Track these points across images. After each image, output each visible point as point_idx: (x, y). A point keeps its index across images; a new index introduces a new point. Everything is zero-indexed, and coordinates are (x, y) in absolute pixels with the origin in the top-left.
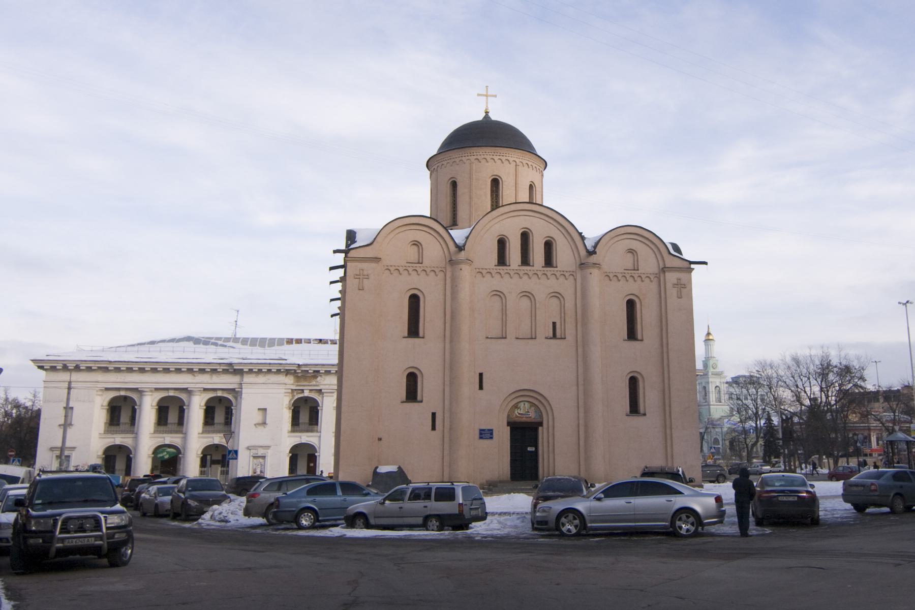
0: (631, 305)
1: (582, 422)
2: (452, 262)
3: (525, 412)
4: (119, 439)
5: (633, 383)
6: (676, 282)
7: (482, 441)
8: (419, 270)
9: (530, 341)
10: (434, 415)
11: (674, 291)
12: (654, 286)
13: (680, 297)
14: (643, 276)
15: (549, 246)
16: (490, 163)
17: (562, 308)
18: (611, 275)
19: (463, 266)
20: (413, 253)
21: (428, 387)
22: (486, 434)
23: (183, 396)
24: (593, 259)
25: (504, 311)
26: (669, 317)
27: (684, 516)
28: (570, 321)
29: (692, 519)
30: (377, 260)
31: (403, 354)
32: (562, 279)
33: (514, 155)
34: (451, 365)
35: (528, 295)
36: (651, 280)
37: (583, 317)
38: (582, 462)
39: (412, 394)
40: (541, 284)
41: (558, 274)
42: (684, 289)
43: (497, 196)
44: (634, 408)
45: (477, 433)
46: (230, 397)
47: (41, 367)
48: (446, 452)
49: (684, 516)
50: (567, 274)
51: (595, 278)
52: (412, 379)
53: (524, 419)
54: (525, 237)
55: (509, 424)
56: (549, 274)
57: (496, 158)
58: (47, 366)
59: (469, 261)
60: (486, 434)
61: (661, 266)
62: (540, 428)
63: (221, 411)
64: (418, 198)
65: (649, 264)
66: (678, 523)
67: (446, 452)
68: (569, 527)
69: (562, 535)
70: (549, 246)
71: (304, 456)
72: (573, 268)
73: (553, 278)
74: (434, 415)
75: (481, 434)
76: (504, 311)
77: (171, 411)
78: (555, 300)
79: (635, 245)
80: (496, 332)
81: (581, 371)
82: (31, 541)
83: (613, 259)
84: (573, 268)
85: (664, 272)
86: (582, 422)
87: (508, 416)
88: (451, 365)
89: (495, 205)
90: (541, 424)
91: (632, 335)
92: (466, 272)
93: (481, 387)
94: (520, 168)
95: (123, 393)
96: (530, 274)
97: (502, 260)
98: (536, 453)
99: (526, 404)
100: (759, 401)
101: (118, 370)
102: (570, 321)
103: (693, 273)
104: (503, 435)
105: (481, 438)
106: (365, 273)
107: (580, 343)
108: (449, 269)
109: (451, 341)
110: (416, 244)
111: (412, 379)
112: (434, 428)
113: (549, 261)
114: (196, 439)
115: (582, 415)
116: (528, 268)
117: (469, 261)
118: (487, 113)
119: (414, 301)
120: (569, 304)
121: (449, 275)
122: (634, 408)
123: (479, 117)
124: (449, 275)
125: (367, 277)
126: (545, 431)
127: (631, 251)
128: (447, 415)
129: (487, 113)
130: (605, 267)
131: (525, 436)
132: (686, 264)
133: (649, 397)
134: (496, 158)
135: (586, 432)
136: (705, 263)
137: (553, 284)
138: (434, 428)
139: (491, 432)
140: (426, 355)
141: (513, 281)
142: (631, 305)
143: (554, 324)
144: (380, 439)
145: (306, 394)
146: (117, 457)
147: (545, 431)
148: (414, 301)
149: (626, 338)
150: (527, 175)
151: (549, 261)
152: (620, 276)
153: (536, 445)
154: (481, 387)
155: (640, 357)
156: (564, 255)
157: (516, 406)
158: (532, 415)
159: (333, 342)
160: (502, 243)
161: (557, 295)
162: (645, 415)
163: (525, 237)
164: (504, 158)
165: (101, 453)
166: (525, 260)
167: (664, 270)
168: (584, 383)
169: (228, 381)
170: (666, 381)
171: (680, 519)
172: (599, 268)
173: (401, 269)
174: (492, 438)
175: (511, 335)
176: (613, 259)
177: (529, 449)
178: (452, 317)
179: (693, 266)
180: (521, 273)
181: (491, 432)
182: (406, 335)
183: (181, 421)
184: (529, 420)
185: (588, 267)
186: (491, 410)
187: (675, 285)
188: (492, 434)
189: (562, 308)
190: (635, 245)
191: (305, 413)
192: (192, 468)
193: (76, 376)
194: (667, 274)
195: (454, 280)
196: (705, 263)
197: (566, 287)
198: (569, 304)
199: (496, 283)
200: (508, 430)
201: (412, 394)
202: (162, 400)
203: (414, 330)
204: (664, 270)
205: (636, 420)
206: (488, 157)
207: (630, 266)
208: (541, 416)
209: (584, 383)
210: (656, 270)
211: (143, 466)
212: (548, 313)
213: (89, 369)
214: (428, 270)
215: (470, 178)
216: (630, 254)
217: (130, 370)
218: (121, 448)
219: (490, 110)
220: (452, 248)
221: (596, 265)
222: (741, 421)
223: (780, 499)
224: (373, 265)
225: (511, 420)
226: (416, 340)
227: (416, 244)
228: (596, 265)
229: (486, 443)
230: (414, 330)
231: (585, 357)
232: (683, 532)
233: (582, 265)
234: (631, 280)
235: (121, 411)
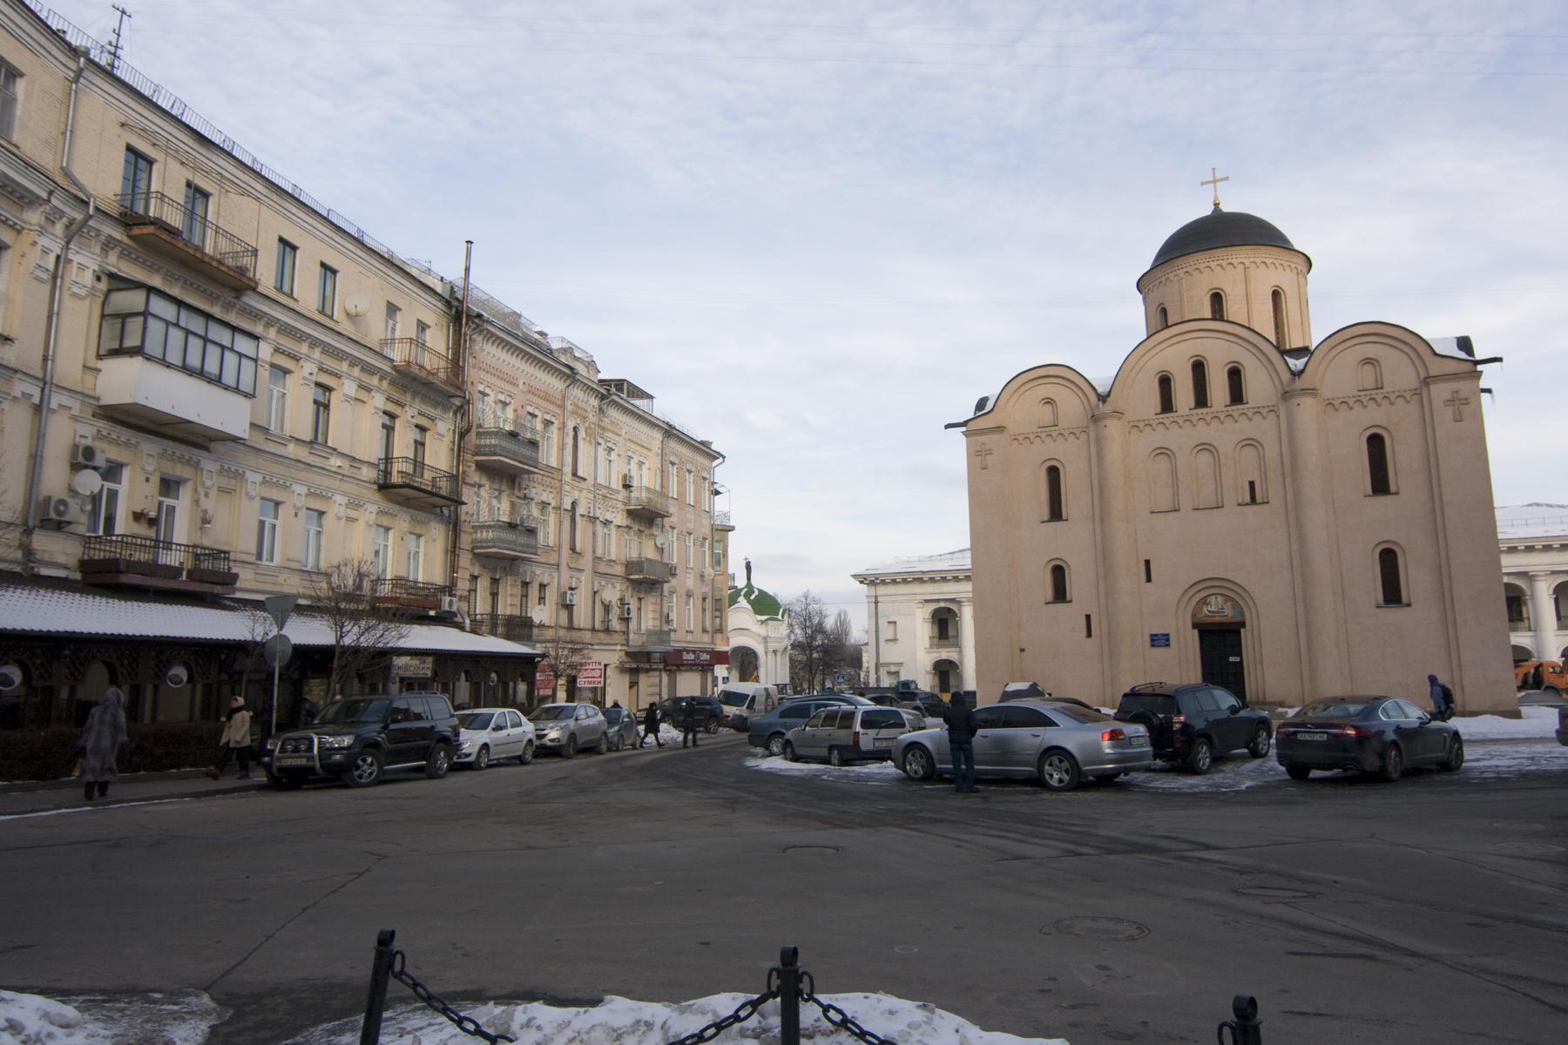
1: (1301, 619)
2: (1095, 419)
6: (1449, 396)
10: (1088, 617)
12: (1413, 408)
14: (1392, 397)
15: (1235, 375)
17: (1261, 458)
18: (1336, 403)
19: (1108, 422)
22: (1161, 640)
25: (1174, 475)
30: (1000, 429)
31: (1042, 543)
32: (1257, 418)
35: (1205, 447)
36: (1424, 395)
37: (1292, 468)
39: (1060, 593)
45: (1148, 639)
50: (1264, 411)
51: (1306, 409)
52: (1059, 573)
53: (1217, 619)
54: (1199, 368)
55: (1195, 626)
56: (1236, 414)
59: (1118, 414)
60: (1161, 640)
61: (1423, 375)
65: (1400, 374)
70: (1235, 375)
72: (1274, 401)
73: (1243, 421)
74: (1088, 617)
76: (1174, 475)
79: (1372, 351)
80: (1167, 505)
83: (1339, 377)
84: (1274, 401)
85: (1428, 384)
87: (1194, 615)
90: (1243, 624)
92: (1113, 428)
93: (1149, 579)
96: (1208, 418)
97: (1167, 405)
98: (1241, 662)
99: (1220, 599)
108: (1092, 427)
110: (1049, 401)
111: (1059, 573)
112: (1089, 635)
113: (1237, 396)
115: (1300, 610)
116: (1205, 410)
120: (1271, 451)
121: (1092, 435)
124: (1092, 435)
127: (1368, 361)
130: (1326, 392)
133: (1414, 578)
135: (1309, 633)
138: (1089, 635)
140: (1071, 542)
141: (1182, 434)
143: (1252, 484)
148: (1054, 474)
149: (1370, 491)
151: (1237, 396)
152: (1351, 402)
154: (1149, 579)
155: (1390, 520)
156: (1258, 385)
157: (1204, 601)
158: (1229, 613)
160: (1165, 382)
161: (1250, 442)
163: (1199, 368)
166: (1201, 400)
167: (1427, 381)
168: (1300, 562)
173: (1032, 437)
176: (1339, 377)
177: (1231, 659)
178: (1100, 489)
179: (1480, 368)
182: (1046, 517)
185: (1293, 397)
187: (1449, 402)
189: (1261, 458)
190: (1372, 351)
195: (1098, 440)
198: (1271, 451)
199: (1160, 437)
201: (1060, 593)
203: (1056, 513)
204: (1427, 381)
205: (1394, 614)
207: (1370, 383)
208: (1242, 614)
209: (1300, 562)
210: (1415, 384)
220: (1093, 398)
221: (1311, 391)
224: (995, 437)
226: (1059, 524)
227: (1049, 401)
228: (1311, 391)
229: (1160, 652)
231: (1300, 526)
233: (1286, 395)
234: (1372, 405)
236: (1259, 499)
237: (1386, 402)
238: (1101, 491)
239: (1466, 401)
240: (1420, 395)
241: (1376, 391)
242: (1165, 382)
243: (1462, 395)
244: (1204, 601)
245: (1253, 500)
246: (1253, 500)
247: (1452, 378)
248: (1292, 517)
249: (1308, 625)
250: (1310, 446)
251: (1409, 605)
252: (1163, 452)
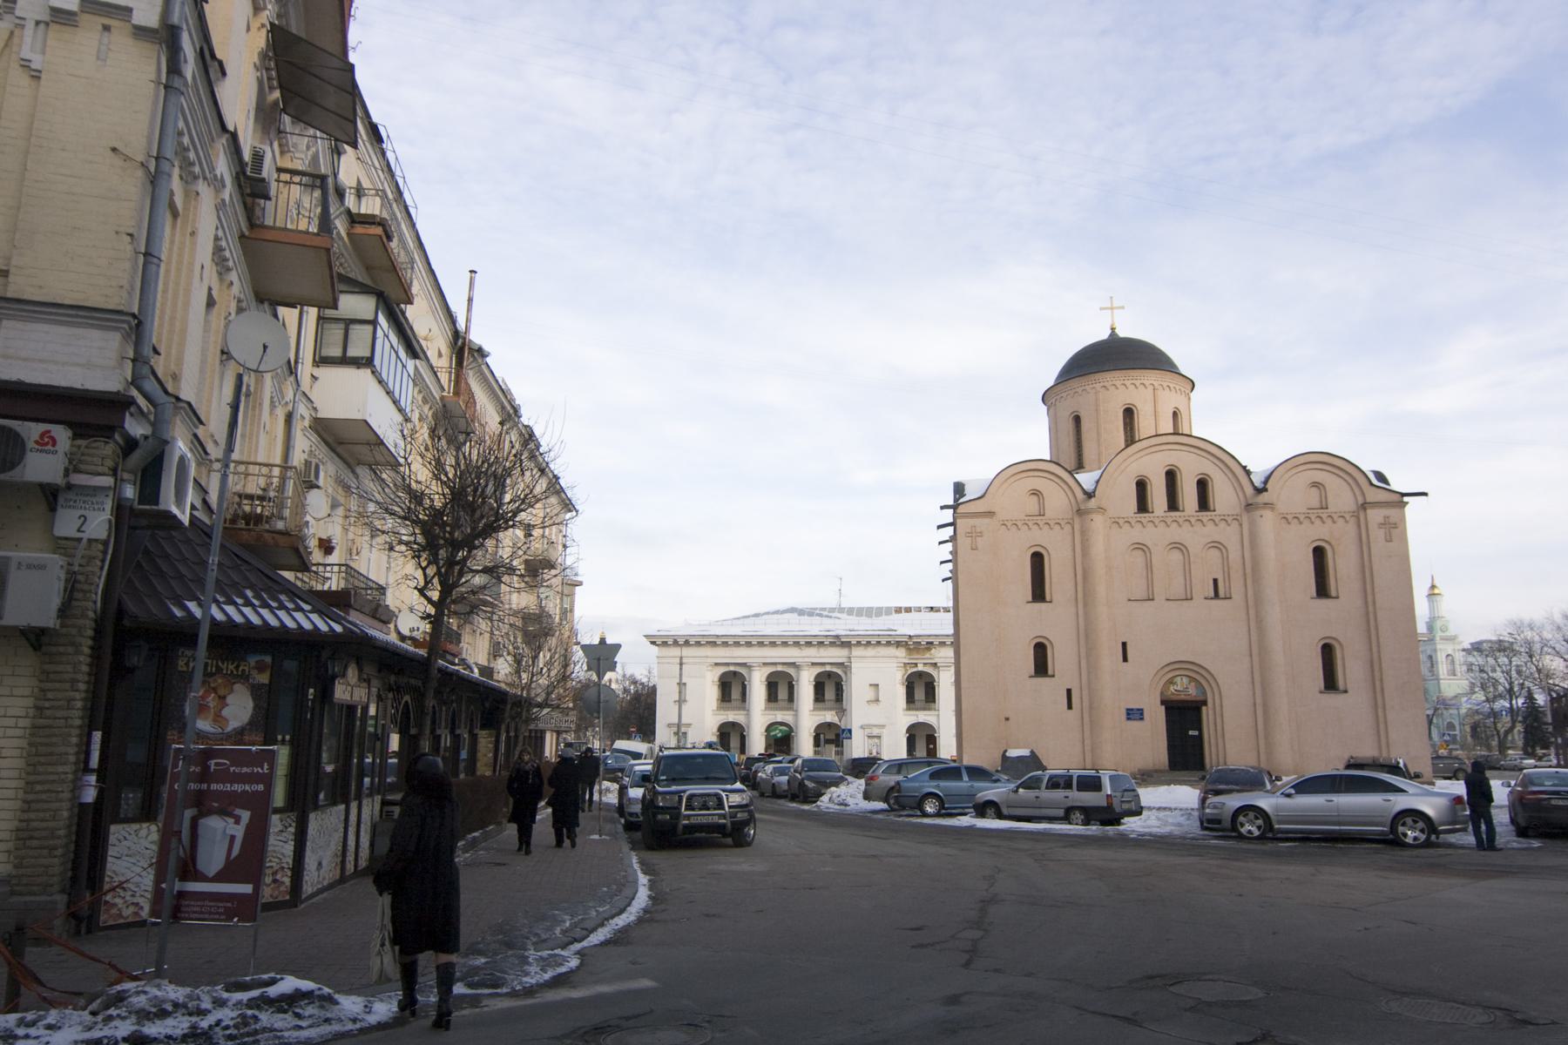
0: (1319, 553)
1: (1259, 701)
2: (1080, 512)
3: (1183, 688)
4: (732, 716)
5: (1328, 651)
9: (1185, 603)
10: (1069, 692)
11: (1381, 533)
12: (1351, 528)
13: (1389, 540)
15: (1202, 485)
16: (1119, 390)
17: (1225, 560)
19: (1093, 516)
20: (1032, 505)
21: (1061, 659)
22: (1134, 714)
23: (791, 671)
24: (1264, 497)
25: (1149, 567)
26: (1375, 568)
27: (1409, 821)
28: (1236, 576)
29: (1421, 825)
30: (990, 514)
32: (1223, 524)
33: (1151, 377)
35: (1178, 546)
36: (1349, 522)
37: (1254, 570)
38: (1262, 750)
39: (1041, 666)
40: (1194, 531)
42: (1395, 530)
43: (1132, 429)
44: (1330, 683)
46: (839, 671)
47: (653, 643)
48: (1087, 733)
49: (1409, 821)
50: (1229, 519)
51: (1267, 522)
52: (1041, 651)
53: (1183, 697)
54: (1171, 476)
55: (1163, 702)
57: (1128, 383)
58: (656, 641)
60: (1134, 714)
61: (1361, 501)
63: (830, 687)
64: (1033, 438)
65: (1342, 498)
66: (1401, 829)
67: (1087, 733)
68: (1250, 827)
69: (1241, 837)
70: (1202, 485)
71: (922, 737)
72: (1238, 511)
73: (1210, 525)
74: (1069, 692)
76: (1149, 567)
77: (780, 687)
78: (1215, 553)
79: (1320, 476)
80: (1142, 594)
81: (1254, 638)
82: (660, 817)
83: (1292, 496)
84: (1238, 511)
86: (1259, 701)
89: (1130, 440)
90: (1205, 703)
91: (1322, 590)
92: (1098, 523)
93: (1125, 659)
94: (1159, 393)
95: (732, 668)
97: (1143, 505)
98: (1200, 738)
99: (1185, 680)
100: (1514, 674)
101: (725, 644)
102: (1236, 576)
103: (1407, 508)
104: (1157, 717)
107: (1251, 603)
109: (1085, 605)
110: (1036, 493)
111: (1041, 651)
112: (1070, 707)
113: (1204, 503)
114: (807, 718)
118: (1113, 329)
119: (1038, 560)
120: (1234, 555)
121: (1077, 527)
122: (1330, 683)
123: (1104, 335)
124: (1077, 527)
125: (981, 534)
127: (1316, 485)
128: (1085, 693)
129: (1113, 329)
130: (1282, 507)
131: (1185, 721)
133: (1351, 669)
134: (1128, 383)
135: (1266, 712)
138: (1070, 707)
139: (1141, 712)
141: (1159, 530)
143: (1215, 581)
145: (920, 668)
146: (730, 733)
148: (1038, 560)
150: (1170, 400)
151: (1204, 503)
153: (1200, 730)
154: (1125, 659)
155: (1336, 618)
156: (1224, 495)
157: (1171, 682)
158: (1192, 693)
159: (946, 610)
160: (1141, 486)
161: (1217, 545)
163: (1171, 476)
164: (1138, 383)
165: (715, 730)
166: (1173, 505)
168: (1259, 652)
169: (835, 655)
170: (1375, 649)
171: (1404, 824)
172: (1273, 509)
178: (1084, 577)
180: (1169, 521)
181: (1141, 712)
183: (791, 698)
186: (1142, 685)
187: (1381, 525)
189: (1225, 560)
190: (1320, 476)
191: (920, 688)
192: (805, 747)
193: (686, 651)
194: (1369, 511)
195: (1083, 532)
197: (1229, 535)
198: (1234, 555)
200: (1161, 711)
201: (1041, 666)
202: (771, 675)
203: (1039, 594)
204: (1364, 506)
205: (1332, 699)
206: (1118, 383)
208: (1205, 693)
209: (1259, 652)
210: (1353, 507)
211: (757, 745)
212: (1207, 567)
213: (698, 644)
215: (1097, 410)
217: (737, 644)
218: (734, 725)
219: (1117, 325)
220: (1080, 495)
221: (1268, 505)
222: (1488, 700)
223: (1553, 802)
224: (986, 520)
227: (1036, 493)
228: (1268, 505)
229: (1135, 725)
230: (1039, 593)
231: (1260, 620)
232: (1409, 840)
233: (1249, 506)
234: (1318, 522)
235: (731, 686)
236: (1221, 594)
237: (1329, 521)
238: (1085, 578)
239: (1395, 526)
242: (1141, 486)
243: (1392, 520)
244: (1171, 682)
245: (1217, 595)
246: (1217, 595)
247: (1378, 502)
248: (1252, 612)
249: (1265, 706)
250: (1269, 553)
252: (1141, 547)
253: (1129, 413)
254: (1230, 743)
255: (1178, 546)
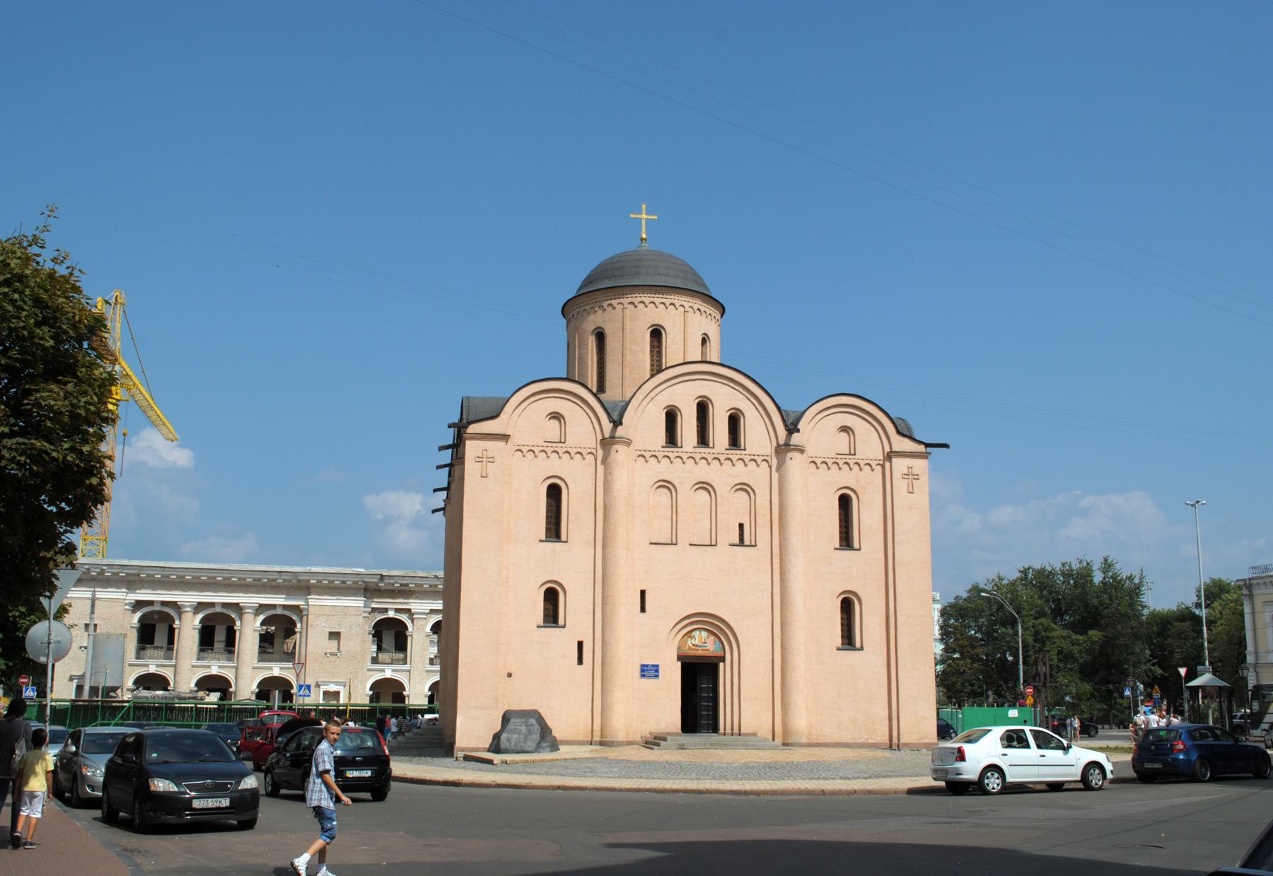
3: (703, 644)
7: (644, 680)
8: (561, 451)
10: (580, 644)
14: (862, 463)
15: (734, 421)
18: (818, 461)
21: (575, 606)
22: (650, 671)
28: (763, 521)
30: (505, 437)
34: (605, 579)
35: (705, 486)
39: (552, 616)
41: (747, 459)
52: (551, 596)
53: (700, 653)
54: (703, 409)
55: (680, 658)
56: (734, 458)
59: (628, 443)
60: (650, 671)
61: (887, 449)
62: (721, 664)
70: (734, 421)
73: (740, 465)
74: (580, 644)
75: (642, 670)
87: (679, 648)
88: (605, 579)
90: (723, 659)
91: (846, 540)
93: (643, 609)
96: (710, 457)
99: (704, 634)
102: (763, 521)
105: (643, 676)
106: (490, 455)
109: (604, 547)
111: (551, 596)
112: (580, 661)
113: (734, 441)
116: (707, 450)
117: (628, 443)
119: (554, 493)
125: (492, 460)
126: (728, 669)
127: (845, 429)
130: (811, 450)
132: (921, 448)
133: (870, 623)
136: (945, 446)
137: (741, 473)
138: (580, 661)
140: (571, 564)
141: (685, 470)
142: (845, 502)
143: (741, 526)
144: (510, 675)
147: (728, 669)
148: (554, 493)
151: (734, 441)
152: (830, 462)
154: (643, 609)
156: (757, 435)
160: (671, 417)
161: (744, 488)
162: (862, 649)
163: (703, 409)
166: (703, 439)
167: (889, 456)
172: (802, 451)
173: (537, 450)
174: (657, 676)
175: (684, 540)
179: (929, 450)
180: (697, 457)
182: (544, 538)
184: (706, 653)
188: (657, 671)
194: (894, 460)
196: (945, 446)
197: (759, 476)
199: (665, 470)
200: (679, 664)
201: (552, 616)
203: (554, 530)
204: (889, 456)
205: (849, 655)
212: (734, 509)
214: (573, 451)
216: (844, 435)
224: (501, 444)
225: (682, 653)
230: (554, 530)
234: (845, 468)
236: (747, 542)
237: (856, 467)
240: (883, 467)
241: (849, 459)
242: (671, 417)
251: (862, 649)
253: (657, 334)
254: (746, 698)
255: (705, 486)
